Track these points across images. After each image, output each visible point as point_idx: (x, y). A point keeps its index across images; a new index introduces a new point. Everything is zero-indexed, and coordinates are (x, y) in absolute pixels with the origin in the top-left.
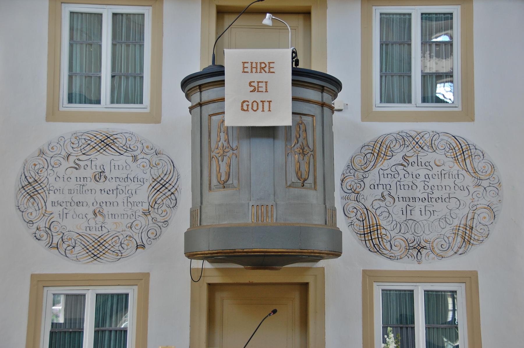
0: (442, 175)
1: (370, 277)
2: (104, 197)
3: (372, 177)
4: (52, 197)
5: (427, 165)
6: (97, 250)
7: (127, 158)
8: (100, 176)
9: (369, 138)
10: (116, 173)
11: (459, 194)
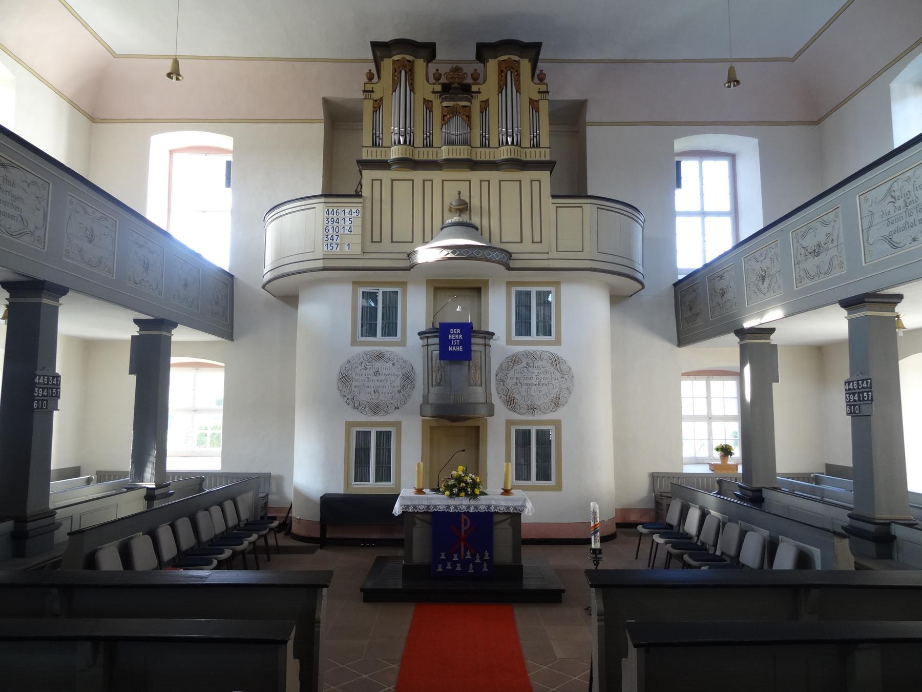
0: (545, 373)
1: (509, 423)
2: (379, 384)
3: (511, 373)
4: (354, 384)
5: (538, 367)
6: (376, 409)
7: (389, 364)
8: (377, 373)
9: (509, 354)
10: (384, 372)
11: (554, 382)
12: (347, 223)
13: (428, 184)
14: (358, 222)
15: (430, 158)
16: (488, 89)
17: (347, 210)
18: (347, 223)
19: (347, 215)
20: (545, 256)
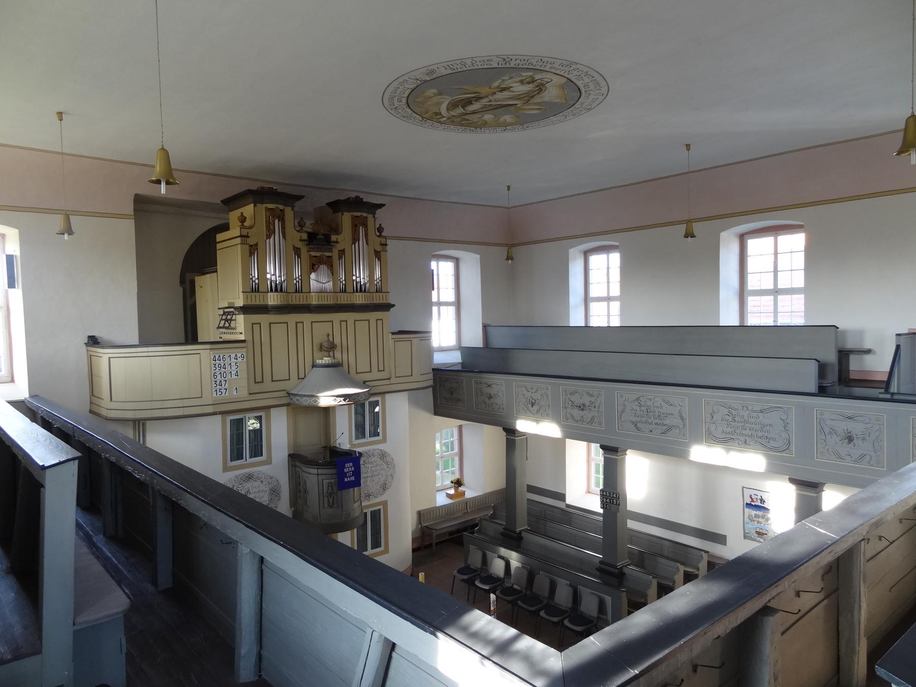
0: (376, 466)
5: (372, 463)
12: (234, 368)
13: (300, 325)
14: (243, 366)
15: (301, 303)
16: (343, 239)
17: (233, 356)
18: (234, 368)
19: (233, 360)
20: (387, 382)
